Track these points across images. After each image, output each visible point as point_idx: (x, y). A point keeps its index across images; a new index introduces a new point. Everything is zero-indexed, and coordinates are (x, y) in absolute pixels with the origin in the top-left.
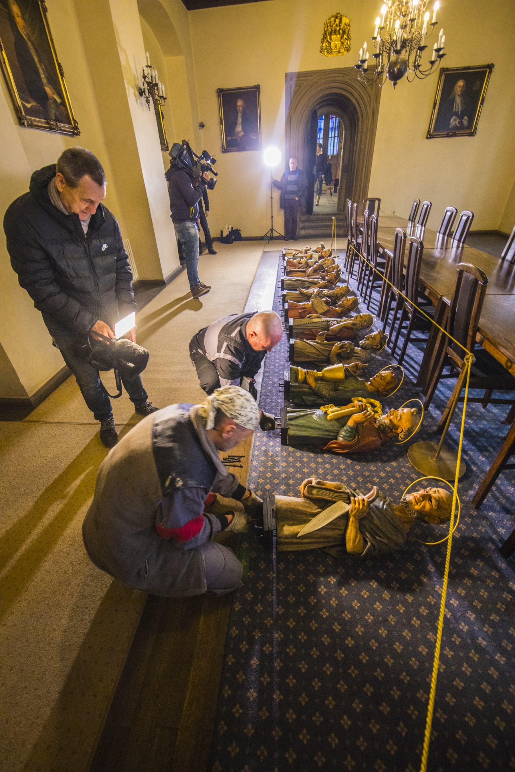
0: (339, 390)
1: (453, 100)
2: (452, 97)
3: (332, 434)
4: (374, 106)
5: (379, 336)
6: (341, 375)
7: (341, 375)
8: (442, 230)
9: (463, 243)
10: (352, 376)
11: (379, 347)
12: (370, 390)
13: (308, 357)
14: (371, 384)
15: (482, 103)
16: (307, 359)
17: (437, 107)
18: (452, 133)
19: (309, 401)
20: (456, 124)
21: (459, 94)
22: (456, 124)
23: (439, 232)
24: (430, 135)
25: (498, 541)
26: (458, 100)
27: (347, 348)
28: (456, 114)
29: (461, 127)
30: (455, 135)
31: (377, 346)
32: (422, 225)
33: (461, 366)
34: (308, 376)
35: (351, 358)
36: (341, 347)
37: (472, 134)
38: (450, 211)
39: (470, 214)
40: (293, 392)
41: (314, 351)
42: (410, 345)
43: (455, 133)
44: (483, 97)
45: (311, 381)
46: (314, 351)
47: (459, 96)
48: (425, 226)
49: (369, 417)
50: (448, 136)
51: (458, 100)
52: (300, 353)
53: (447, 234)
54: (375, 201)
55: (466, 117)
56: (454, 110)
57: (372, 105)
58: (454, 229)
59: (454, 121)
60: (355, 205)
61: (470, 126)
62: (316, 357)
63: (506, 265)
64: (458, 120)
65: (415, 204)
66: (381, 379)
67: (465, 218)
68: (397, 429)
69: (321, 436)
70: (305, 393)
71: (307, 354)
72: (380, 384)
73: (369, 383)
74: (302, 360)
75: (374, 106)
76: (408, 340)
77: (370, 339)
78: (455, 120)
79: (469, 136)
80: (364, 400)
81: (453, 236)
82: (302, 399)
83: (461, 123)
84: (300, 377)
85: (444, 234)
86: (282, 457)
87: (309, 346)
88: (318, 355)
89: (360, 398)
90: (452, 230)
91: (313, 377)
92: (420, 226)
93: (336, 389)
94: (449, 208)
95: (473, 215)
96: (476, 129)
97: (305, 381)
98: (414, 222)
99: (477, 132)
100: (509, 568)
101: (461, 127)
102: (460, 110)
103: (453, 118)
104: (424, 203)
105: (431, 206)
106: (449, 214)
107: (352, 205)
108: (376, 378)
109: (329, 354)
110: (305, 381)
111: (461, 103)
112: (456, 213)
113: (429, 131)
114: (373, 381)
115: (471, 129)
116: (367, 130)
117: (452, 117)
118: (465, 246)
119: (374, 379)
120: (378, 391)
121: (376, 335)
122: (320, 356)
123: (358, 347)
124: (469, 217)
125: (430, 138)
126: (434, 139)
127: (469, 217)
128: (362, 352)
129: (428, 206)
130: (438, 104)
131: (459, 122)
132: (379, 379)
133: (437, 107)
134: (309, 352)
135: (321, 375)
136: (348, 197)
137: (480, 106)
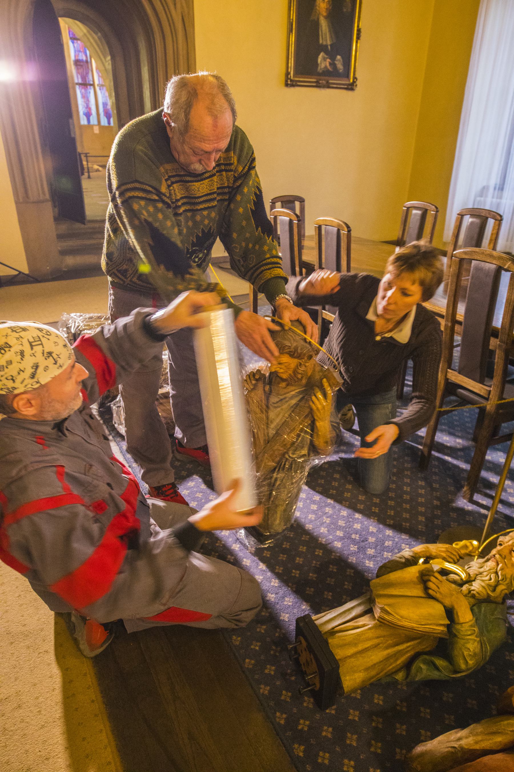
1: (316, 25)
2: (312, 18)
4: (182, 7)
15: (358, 38)
18: (324, 80)
20: (326, 67)
21: (325, 14)
22: (326, 67)
24: (291, 81)
26: (324, 24)
28: (324, 48)
29: (333, 73)
30: (328, 86)
37: (351, 87)
43: (327, 82)
44: (358, 26)
47: (326, 18)
50: (318, 86)
51: (324, 24)
55: (339, 57)
56: (321, 42)
57: (178, 6)
59: (323, 62)
64: (328, 60)
75: (182, 7)
78: (324, 59)
83: (333, 64)
96: (355, 78)
99: (358, 83)
101: (333, 73)
102: (329, 43)
111: (330, 31)
113: (287, 74)
115: (348, 77)
117: (319, 55)
125: (292, 86)
126: (297, 89)
131: (330, 64)
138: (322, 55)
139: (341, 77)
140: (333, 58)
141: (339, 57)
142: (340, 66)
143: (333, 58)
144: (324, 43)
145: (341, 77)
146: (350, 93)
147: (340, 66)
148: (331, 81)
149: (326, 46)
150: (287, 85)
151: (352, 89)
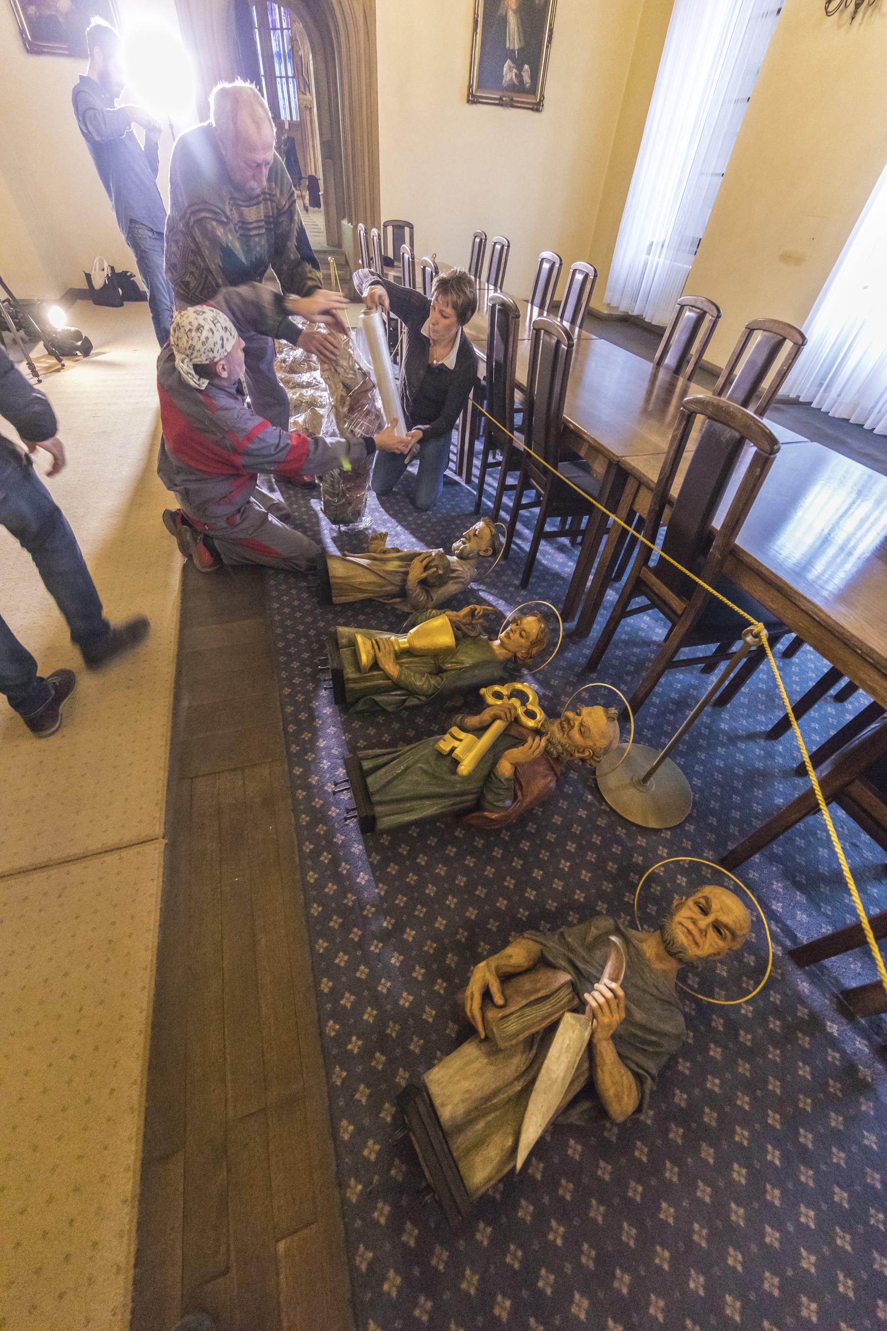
0: (446, 671)
1: (504, 20)
2: (501, 12)
3: (470, 797)
5: (487, 531)
6: (447, 639)
7: (447, 639)
8: (538, 299)
9: (581, 327)
10: (466, 636)
11: (490, 553)
12: (501, 658)
13: (361, 591)
14: (502, 645)
15: (549, 42)
16: (361, 596)
17: (479, 30)
19: (390, 704)
20: (512, 79)
21: (514, 7)
22: (512, 79)
23: (532, 303)
24: (473, 96)
25: (781, 934)
27: (437, 567)
28: (510, 54)
30: (511, 104)
31: (486, 551)
32: (495, 285)
33: (680, 612)
34: (380, 655)
35: (446, 583)
36: (426, 568)
37: (537, 107)
38: (548, 260)
39: (590, 269)
40: (352, 690)
41: (372, 578)
42: (544, 546)
43: (512, 100)
44: (550, 25)
45: (391, 667)
46: (372, 578)
47: (515, 12)
48: (501, 288)
49: (537, 752)
50: (501, 103)
52: (345, 587)
53: (546, 308)
54: (403, 227)
56: (508, 45)
58: (560, 296)
59: (509, 73)
60: (375, 231)
61: (533, 91)
62: (378, 589)
63: (662, 375)
64: (515, 70)
65: (478, 240)
66: (521, 635)
67: (579, 277)
68: (583, 752)
69: (449, 809)
70: (379, 690)
71: (359, 587)
72: (521, 646)
73: (498, 642)
74: (350, 598)
76: (540, 535)
77: (472, 539)
79: (532, 109)
80: (504, 690)
81: (560, 314)
82: (376, 703)
83: (519, 76)
84: (364, 659)
85: (542, 307)
86: (374, 868)
87: (360, 571)
88: (382, 586)
89: (497, 688)
90: (555, 299)
91: (392, 655)
92: (492, 287)
93: (439, 671)
94: (546, 254)
95: (595, 271)
96: (542, 96)
97: (375, 665)
98: (480, 278)
99: (545, 102)
100: (814, 989)
101: (518, 88)
102: (517, 47)
103: (506, 65)
104: (495, 239)
105: (509, 246)
106: (546, 266)
107: (367, 232)
108: (511, 635)
109: (405, 581)
110: (375, 665)
112: (561, 264)
113: (470, 86)
114: (505, 640)
116: (359, 60)
118: (584, 332)
119: (508, 636)
120: (515, 657)
121: (481, 530)
122: (384, 586)
123: (452, 554)
124: (587, 275)
125: (474, 102)
126: (480, 106)
127: (587, 275)
128: (461, 566)
129: (503, 247)
130: (480, 20)
132: (517, 635)
133: (479, 30)
134: (361, 583)
135: (407, 645)
136: (344, 217)
137: (547, 47)
138: (508, 63)
139: (527, 95)
140: (520, 68)
141: (526, 67)
142: (527, 79)
143: (520, 68)
144: (511, 48)
145: (527, 95)
146: (536, 114)
147: (527, 79)
148: (515, 99)
149: (514, 51)
150: (468, 101)
151: (538, 110)
